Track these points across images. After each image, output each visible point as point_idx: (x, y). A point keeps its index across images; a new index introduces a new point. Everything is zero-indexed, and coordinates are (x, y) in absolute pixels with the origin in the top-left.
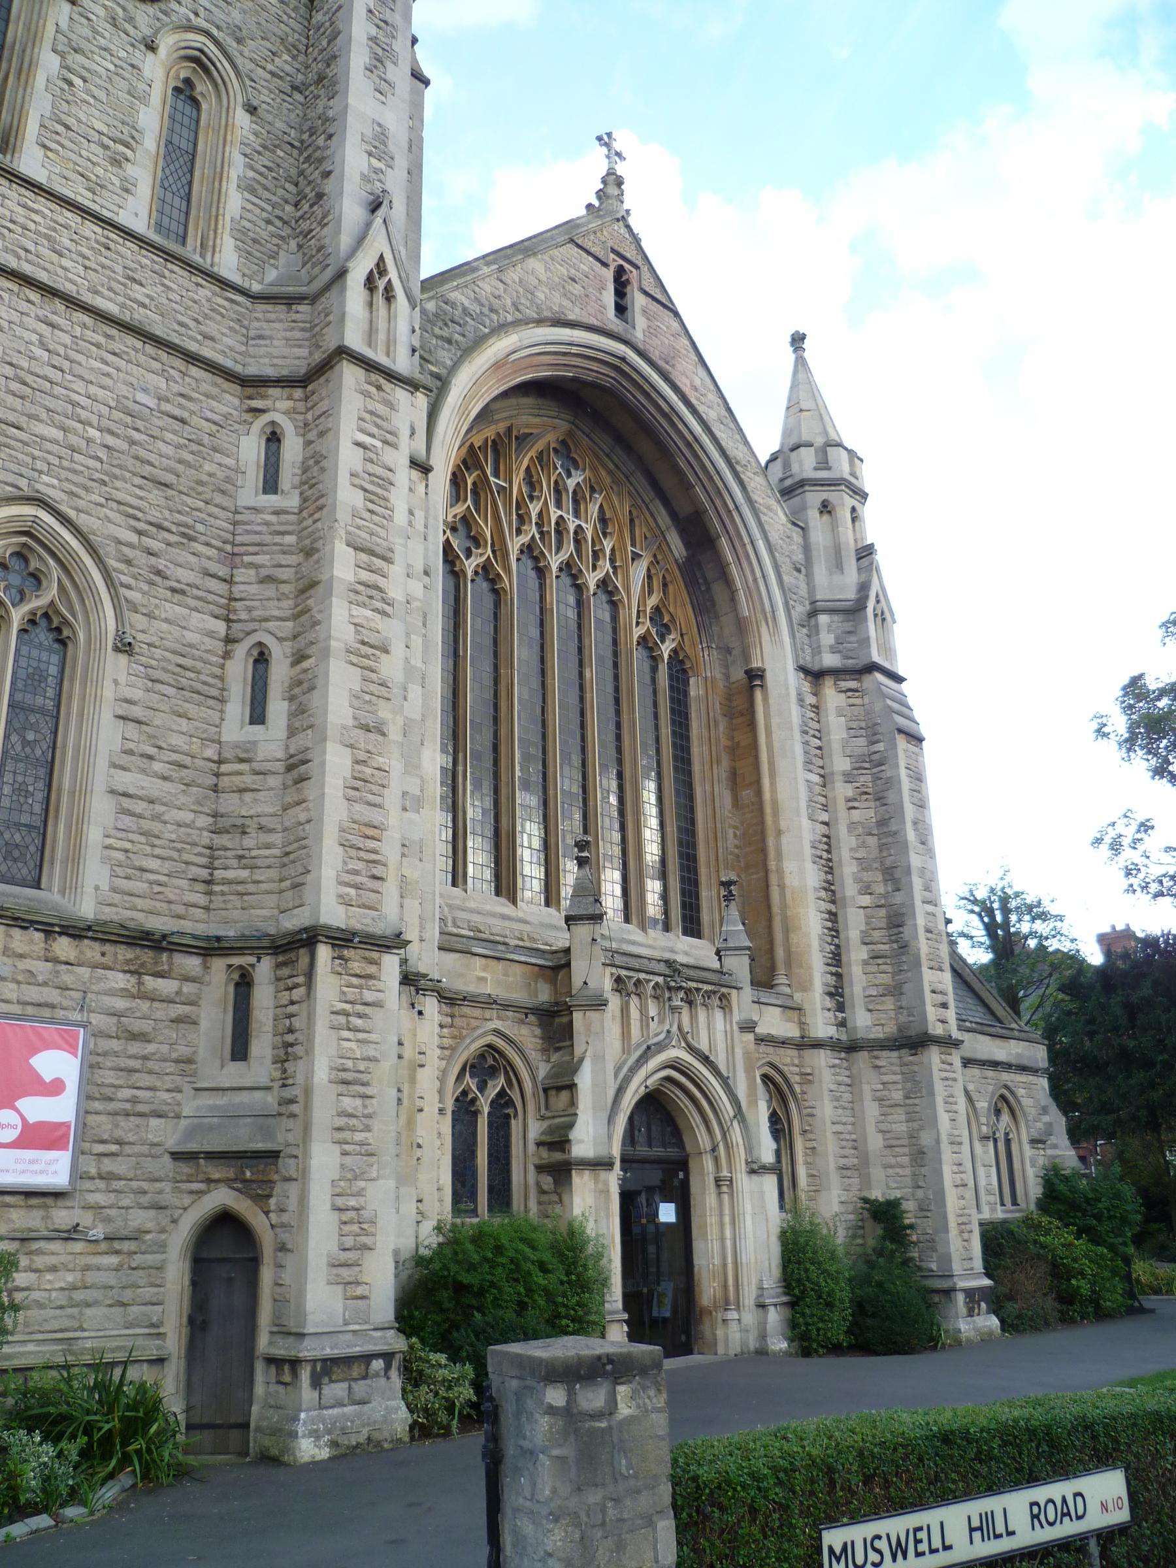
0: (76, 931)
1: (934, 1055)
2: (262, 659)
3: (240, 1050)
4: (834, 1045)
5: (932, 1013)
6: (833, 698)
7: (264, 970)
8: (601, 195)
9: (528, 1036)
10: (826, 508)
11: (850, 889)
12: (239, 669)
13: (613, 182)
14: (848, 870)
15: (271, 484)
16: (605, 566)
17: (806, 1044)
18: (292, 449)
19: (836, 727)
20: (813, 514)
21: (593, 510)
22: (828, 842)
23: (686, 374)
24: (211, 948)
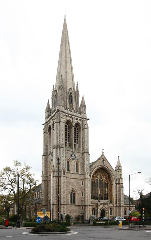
0: (76, 205)
1: (121, 207)
2: (83, 193)
3: (83, 209)
4: (115, 206)
5: (121, 205)
6: (118, 185)
7: (84, 206)
8: (102, 154)
9: (96, 207)
10: (119, 171)
11: (117, 197)
12: (82, 193)
13: (103, 152)
14: (117, 196)
15: (83, 184)
16: (102, 178)
17: (114, 206)
18: (83, 183)
19: (118, 187)
20: (118, 172)
21: (101, 175)
22: (116, 194)
23: (108, 165)
24: (81, 205)
